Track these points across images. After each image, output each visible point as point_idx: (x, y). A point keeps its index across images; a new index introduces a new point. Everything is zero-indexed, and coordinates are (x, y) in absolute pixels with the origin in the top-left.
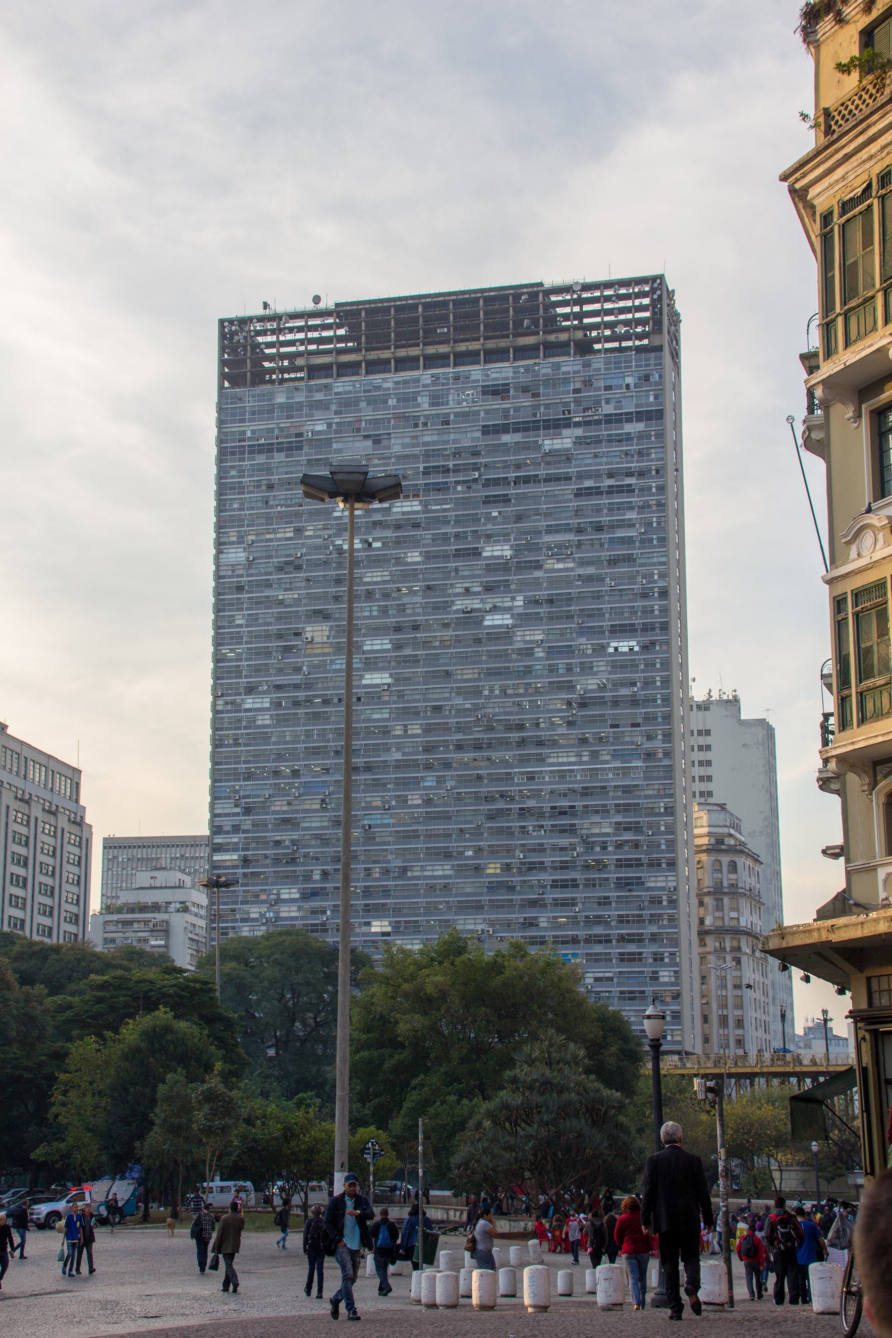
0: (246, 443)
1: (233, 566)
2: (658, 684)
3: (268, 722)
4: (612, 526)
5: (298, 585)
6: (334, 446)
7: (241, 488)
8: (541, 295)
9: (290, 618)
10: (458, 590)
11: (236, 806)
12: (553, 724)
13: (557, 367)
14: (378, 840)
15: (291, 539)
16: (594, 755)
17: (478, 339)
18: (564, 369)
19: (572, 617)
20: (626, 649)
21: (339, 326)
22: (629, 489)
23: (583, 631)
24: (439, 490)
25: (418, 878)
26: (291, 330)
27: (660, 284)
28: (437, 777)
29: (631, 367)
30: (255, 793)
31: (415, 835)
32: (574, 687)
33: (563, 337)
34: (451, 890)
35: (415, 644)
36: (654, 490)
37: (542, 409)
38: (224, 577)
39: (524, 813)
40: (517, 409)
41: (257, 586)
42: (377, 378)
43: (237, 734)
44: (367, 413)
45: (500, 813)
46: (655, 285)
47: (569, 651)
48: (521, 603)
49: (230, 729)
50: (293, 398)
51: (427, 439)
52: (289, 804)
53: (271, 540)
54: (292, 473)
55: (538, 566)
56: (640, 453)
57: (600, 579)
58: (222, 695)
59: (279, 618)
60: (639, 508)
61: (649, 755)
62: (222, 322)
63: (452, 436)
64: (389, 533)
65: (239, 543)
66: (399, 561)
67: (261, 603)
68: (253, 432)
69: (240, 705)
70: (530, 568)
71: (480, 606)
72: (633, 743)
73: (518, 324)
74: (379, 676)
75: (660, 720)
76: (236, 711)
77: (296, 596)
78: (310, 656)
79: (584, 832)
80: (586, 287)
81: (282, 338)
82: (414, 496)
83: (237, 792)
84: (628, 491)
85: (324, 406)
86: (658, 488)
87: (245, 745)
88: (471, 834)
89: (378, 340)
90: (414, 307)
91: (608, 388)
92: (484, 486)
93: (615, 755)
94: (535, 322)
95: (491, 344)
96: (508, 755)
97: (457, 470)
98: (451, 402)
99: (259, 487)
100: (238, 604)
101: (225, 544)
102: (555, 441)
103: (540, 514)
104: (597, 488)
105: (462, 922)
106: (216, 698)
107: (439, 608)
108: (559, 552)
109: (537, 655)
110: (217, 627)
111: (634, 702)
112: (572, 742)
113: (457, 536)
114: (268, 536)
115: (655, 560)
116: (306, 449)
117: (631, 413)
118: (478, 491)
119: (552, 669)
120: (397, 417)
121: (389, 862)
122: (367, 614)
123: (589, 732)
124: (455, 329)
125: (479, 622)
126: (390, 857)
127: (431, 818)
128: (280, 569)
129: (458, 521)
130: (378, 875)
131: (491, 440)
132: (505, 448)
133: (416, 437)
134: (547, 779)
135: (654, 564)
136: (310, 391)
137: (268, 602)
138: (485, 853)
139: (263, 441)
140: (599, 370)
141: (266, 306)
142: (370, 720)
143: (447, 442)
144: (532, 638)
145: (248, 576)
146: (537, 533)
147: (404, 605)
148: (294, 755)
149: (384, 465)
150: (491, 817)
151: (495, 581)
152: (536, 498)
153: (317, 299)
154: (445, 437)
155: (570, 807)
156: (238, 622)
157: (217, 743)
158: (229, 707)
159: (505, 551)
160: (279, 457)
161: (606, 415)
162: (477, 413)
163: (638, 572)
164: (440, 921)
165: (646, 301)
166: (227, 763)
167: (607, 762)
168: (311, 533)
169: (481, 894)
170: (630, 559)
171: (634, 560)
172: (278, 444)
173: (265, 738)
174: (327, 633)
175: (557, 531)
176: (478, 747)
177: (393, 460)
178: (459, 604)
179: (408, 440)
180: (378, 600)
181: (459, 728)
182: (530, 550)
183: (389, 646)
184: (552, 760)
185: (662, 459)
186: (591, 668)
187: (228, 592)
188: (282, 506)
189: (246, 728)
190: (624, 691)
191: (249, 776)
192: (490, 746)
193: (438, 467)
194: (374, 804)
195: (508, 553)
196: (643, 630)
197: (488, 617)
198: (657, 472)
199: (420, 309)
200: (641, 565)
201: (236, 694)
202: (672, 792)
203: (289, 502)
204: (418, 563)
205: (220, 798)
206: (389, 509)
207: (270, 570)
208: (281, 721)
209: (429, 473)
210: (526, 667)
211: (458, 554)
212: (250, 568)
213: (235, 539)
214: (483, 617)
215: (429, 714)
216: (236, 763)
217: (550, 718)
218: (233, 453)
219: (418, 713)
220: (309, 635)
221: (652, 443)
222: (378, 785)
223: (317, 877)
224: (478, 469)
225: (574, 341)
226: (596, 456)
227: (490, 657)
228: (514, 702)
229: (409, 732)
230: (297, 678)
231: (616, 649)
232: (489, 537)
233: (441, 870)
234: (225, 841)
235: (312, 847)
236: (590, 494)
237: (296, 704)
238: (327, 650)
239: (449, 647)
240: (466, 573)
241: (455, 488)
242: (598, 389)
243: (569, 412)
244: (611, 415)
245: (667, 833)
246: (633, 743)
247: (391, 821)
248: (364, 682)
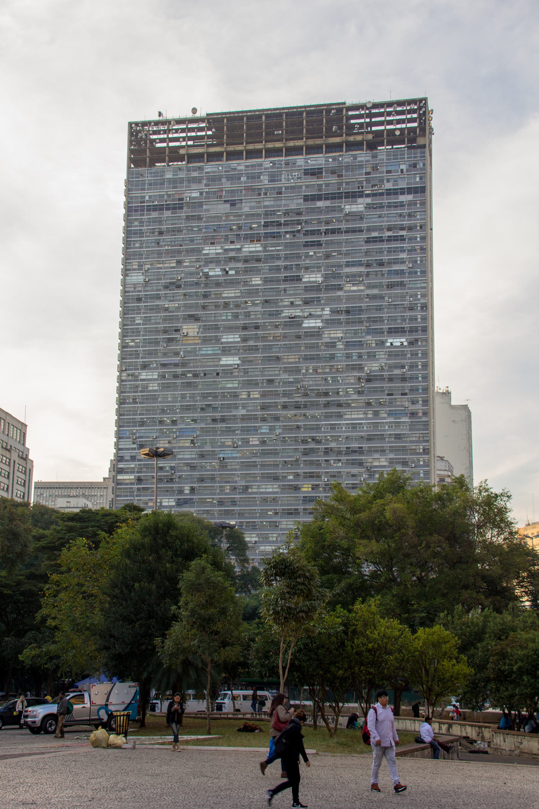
0: (145, 204)
1: (135, 285)
2: (420, 367)
3: (156, 388)
4: (390, 263)
5: (178, 298)
6: (204, 207)
7: (141, 233)
8: (344, 110)
9: (172, 319)
10: (286, 303)
11: (134, 443)
12: (347, 392)
13: (355, 157)
14: (229, 467)
15: (174, 267)
16: (376, 414)
17: (302, 139)
18: (359, 159)
19: (362, 322)
20: (399, 344)
21: (209, 129)
22: (402, 239)
23: (369, 332)
24: (274, 237)
25: (256, 493)
26: (177, 131)
27: (425, 104)
28: (270, 426)
29: (404, 158)
30: (146, 435)
31: (254, 465)
32: (363, 368)
33: (359, 138)
34: (278, 501)
35: (256, 338)
36: (418, 239)
37: (344, 184)
38: (129, 292)
39: (327, 451)
40: (327, 185)
41: (151, 298)
42: (234, 163)
43: (135, 396)
44: (227, 185)
45: (312, 450)
46: (422, 105)
47: (360, 344)
48: (328, 313)
49: (131, 392)
50: (177, 175)
51: (266, 203)
52: (169, 443)
53: (161, 268)
54: (176, 224)
55: (340, 288)
56: (410, 215)
57: (382, 297)
58: (126, 370)
59: (165, 319)
60: (409, 251)
61: (413, 414)
62: (130, 124)
63: (283, 202)
64: (240, 265)
65: (139, 269)
66: (246, 283)
67: (153, 309)
68: (150, 197)
69: (137, 376)
70: (335, 289)
71: (301, 314)
72: (402, 406)
73: (329, 129)
74: (232, 359)
75: (420, 391)
76: (135, 381)
77: (177, 305)
78: (185, 345)
79: (368, 464)
80: (376, 106)
81: (170, 136)
82: (257, 241)
83: (134, 434)
84: (401, 240)
85: (198, 180)
86: (421, 238)
87: (141, 403)
88: (292, 465)
90: (260, 117)
91: (389, 172)
92: (304, 235)
93: (390, 414)
94: (341, 128)
95: (311, 142)
96: (317, 413)
97: (286, 224)
98: (283, 180)
99: (153, 233)
100: (138, 310)
101: (130, 270)
102: (352, 206)
103: (342, 254)
104: (380, 237)
105: (285, 523)
106: (121, 371)
107: (273, 315)
108: (353, 278)
109: (338, 347)
110: (123, 325)
111: (404, 379)
112: (361, 405)
113: (286, 268)
114: (159, 266)
115: (419, 285)
116: (185, 209)
117: (404, 189)
118: (301, 238)
119: (348, 356)
120: (247, 189)
121: (236, 482)
122: (224, 318)
123: (372, 398)
125: (300, 324)
126: (237, 479)
127: (264, 453)
128: (166, 287)
129: (286, 258)
130: (228, 491)
131: (310, 205)
132: (319, 210)
133: (259, 202)
134: (344, 429)
135: (418, 288)
136: (188, 171)
137: (157, 309)
138: (301, 477)
139: (156, 203)
140: (383, 160)
141: (160, 114)
142: (225, 388)
143: (280, 206)
144: (335, 335)
145: (144, 291)
146: (340, 266)
147: (249, 312)
148: (172, 410)
149: (237, 220)
150: (306, 453)
151: (310, 298)
152: (339, 243)
153: (194, 111)
154: (279, 203)
155: (359, 448)
156: (137, 322)
157: (121, 402)
158: (130, 378)
159: (317, 278)
160: (168, 214)
161: (387, 190)
162: (301, 187)
163: (407, 293)
164: (270, 522)
165: (415, 116)
166: (128, 415)
167: (384, 418)
168: (188, 264)
169: (299, 505)
170: (401, 284)
171: (405, 285)
172: (166, 205)
173: (154, 399)
174: (197, 330)
175: (353, 266)
176: (298, 407)
177: (243, 217)
178: (287, 313)
179: (254, 204)
180: (232, 309)
181: (285, 394)
182: (334, 278)
183: (239, 340)
184: (347, 417)
185: (424, 219)
186: (375, 356)
187: (131, 303)
188: (168, 245)
189: (141, 392)
190: (397, 372)
191: (142, 423)
192: (305, 406)
193: (274, 222)
194: (227, 444)
195: (320, 280)
196: (410, 331)
197: (305, 322)
198: (421, 227)
199: (264, 118)
200: (409, 289)
201: (135, 369)
202: (428, 439)
203: (173, 243)
204: (259, 285)
205: (123, 438)
206: (240, 250)
207: (160, 288)
208: (165, 387)
209: (267, 226)
210: (331, 354)
211: (286, 279)
212: (146, 286)
213: (136, 267)
214: (302, 321)
215: (265, 384)
216: (134, 415)
217: (347, 388)
218: (136, 211)
219: (258, 384)
220: (185, 331)
221: (418, 208)
222: (230, 431)
223: (187, 492)
224: (301, 224)
225: (367, 141)
226: (380, 217)
227: (306, 348)
228: (322, 378)
229: (251, 396)
230: (176, 360)
231: (391, 344)
232: (307, 268)
233: (271, 488)
234: (125, 466)
235: (185, 471)
236: (376, 241)
237: (176, 376)
238: (197, 341)
239: (279, 341)
240: (292, 292)
241: (285, 236)
242: (383, 172)
243: (362, 187)
244: (390, 189)
245: (424, 466)
246: (402, 406)
247: (238, 455)
248: (222, 363)
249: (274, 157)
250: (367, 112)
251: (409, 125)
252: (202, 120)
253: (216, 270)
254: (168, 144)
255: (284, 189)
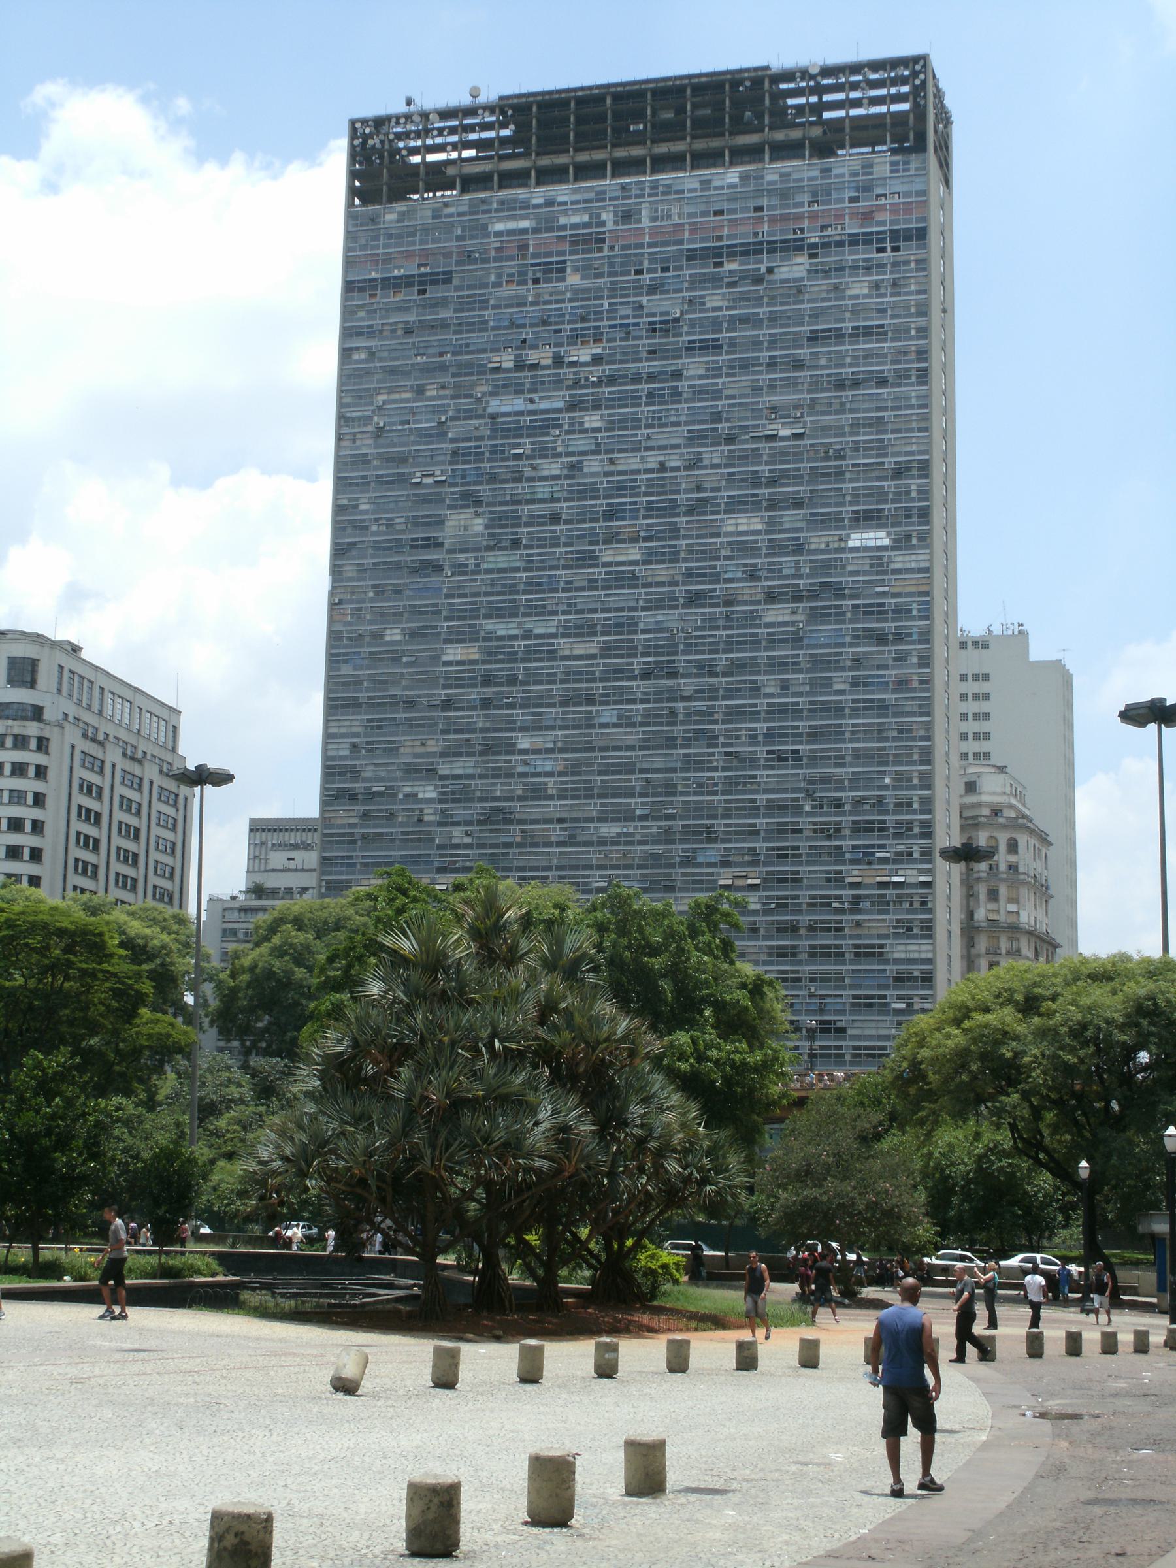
33: (796, 134)
80: (827, 71)
81: (429, 142)
89: (552, 142)
90: (600, 99)
124: (653, 126)
161: (850, 235)
165: (905, 89)
243: (802, 230)
249: (629, 175)
250: (812, 83)
251: (895, 108)
252: (490, 109)
254: (424, 158)
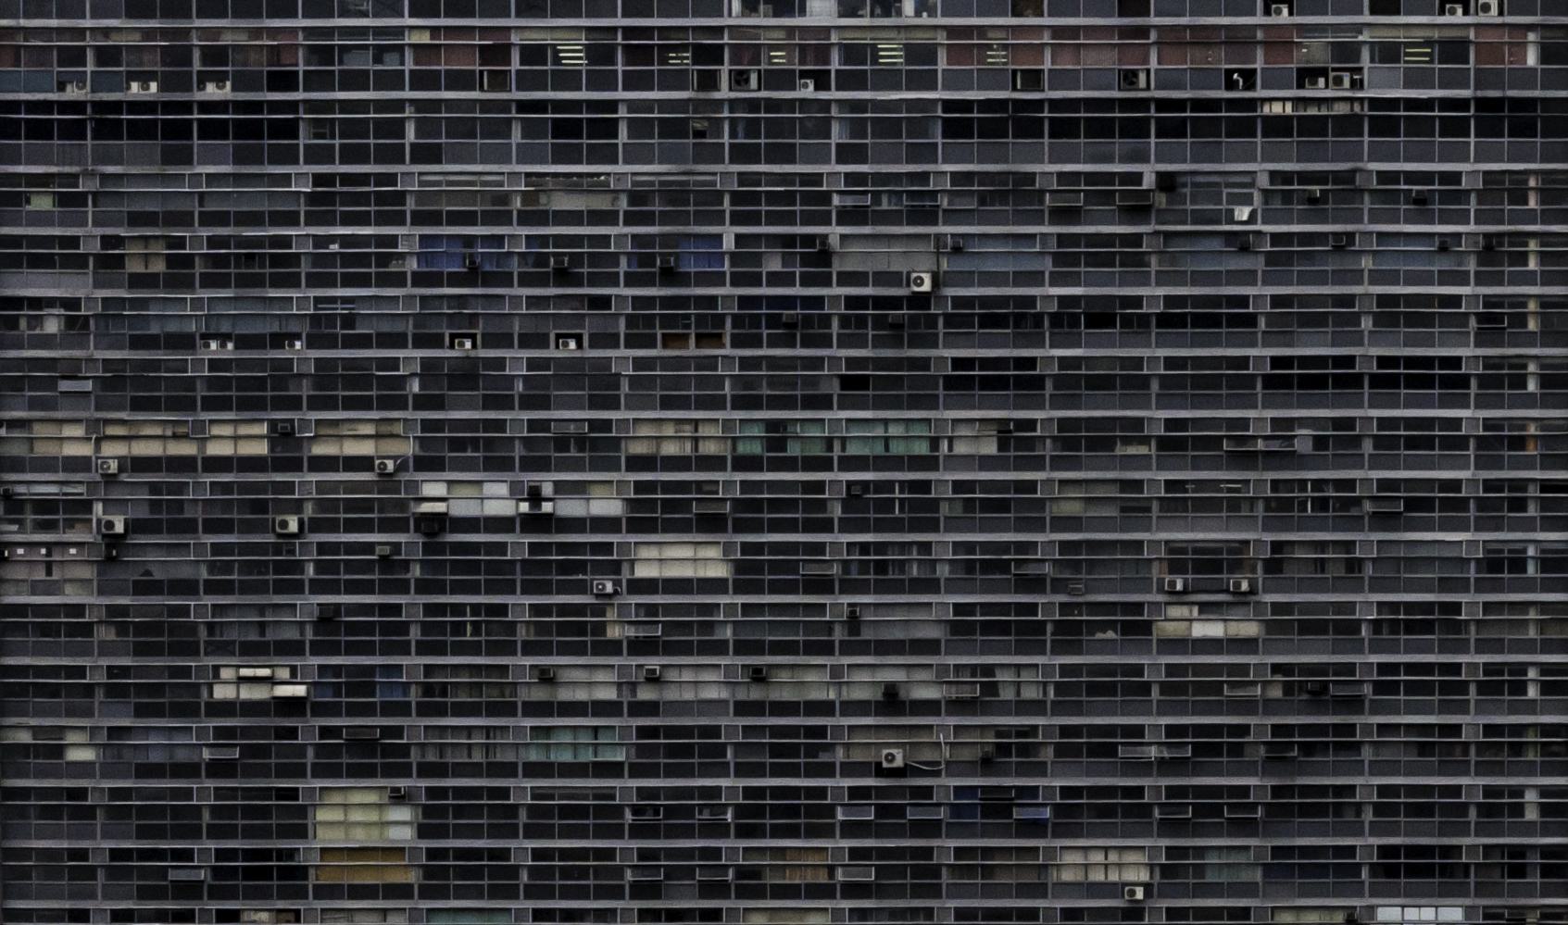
22: (1450, 380)
117: (1461, 104)
144: (1114, 877)
188: (223, 338)
243: (1249, 76)
253: (490, 489)
255: (835, 65)
